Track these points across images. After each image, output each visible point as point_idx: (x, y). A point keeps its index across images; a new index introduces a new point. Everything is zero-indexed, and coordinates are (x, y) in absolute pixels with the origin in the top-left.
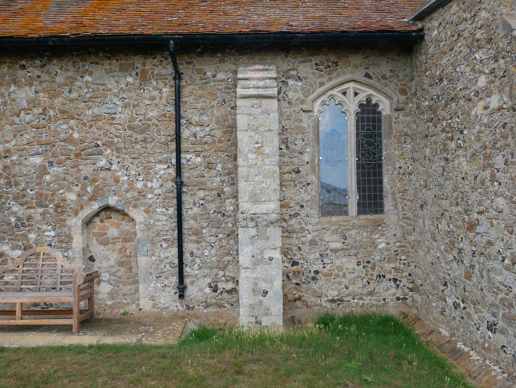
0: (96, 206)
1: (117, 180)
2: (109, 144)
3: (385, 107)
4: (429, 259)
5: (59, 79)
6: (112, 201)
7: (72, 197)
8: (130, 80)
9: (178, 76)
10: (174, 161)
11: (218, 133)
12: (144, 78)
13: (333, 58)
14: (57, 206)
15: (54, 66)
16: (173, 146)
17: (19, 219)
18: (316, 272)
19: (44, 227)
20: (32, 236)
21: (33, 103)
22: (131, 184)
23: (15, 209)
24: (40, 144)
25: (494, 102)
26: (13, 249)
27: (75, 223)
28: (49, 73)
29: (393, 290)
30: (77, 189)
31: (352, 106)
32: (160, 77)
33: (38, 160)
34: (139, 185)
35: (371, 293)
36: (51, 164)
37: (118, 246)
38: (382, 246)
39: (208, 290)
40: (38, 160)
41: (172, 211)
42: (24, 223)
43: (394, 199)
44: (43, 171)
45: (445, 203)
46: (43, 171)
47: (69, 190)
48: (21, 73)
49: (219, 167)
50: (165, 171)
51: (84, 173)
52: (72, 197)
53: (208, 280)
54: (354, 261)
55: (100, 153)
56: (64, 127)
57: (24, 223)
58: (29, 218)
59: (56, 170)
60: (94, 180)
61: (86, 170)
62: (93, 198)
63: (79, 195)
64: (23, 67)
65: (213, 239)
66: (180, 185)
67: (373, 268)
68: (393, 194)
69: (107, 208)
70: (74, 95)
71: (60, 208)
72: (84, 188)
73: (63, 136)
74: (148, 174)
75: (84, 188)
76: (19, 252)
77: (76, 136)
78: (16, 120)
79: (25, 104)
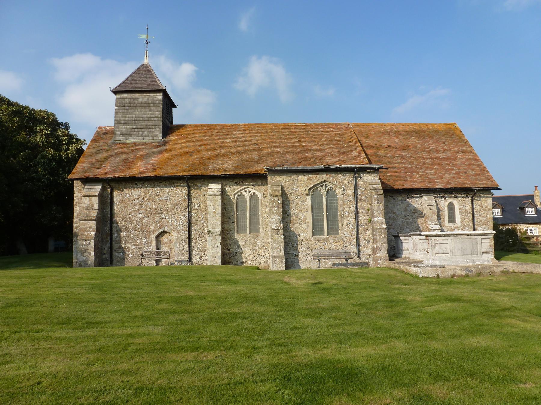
0: (160, 231)
1: (168, 222)
6: (166, 229)
7: (152, 228)
9: (189, 187)
10: (187, 215)
13: (241, 180)
14: (147, 231)
17: (134, 236)
18: (236, 253)
19: (143, 238)
20: (138, 241)
21: (140, 196)
23: (133, 232)
26: (132, 246)
29: (263, 259)
33: (141, 215)
34: (175, 224)
35: (255, 260)
36: (145, 217)
37: (168, 245)
38: (258, 244)
39: (199, 259)
40: (141, 215)
41: (187, 232)
42: (136, 237)
43: (263, 227)
44: (142, 219)
47: (151, 225)
50: (184, 219)
51: (156, 220)
52: (152, 228)
53: (198, 256)
54: (249, 249)
55: (162, 213)
56: (150, 204)
57: (136, 237)
58: (138, 235)
59: (146, 219)
60: (159, 222)
62: (160, 228)
65: (200, 242)
67: (256, 251)
68: (262, 226)
71: (148, 231)
72: (156, 225)
74: (178, 219)
75: (156, 225)
76: (134, 247)
77: (154, 207)
78: (134, 202)
79: (136, 197)
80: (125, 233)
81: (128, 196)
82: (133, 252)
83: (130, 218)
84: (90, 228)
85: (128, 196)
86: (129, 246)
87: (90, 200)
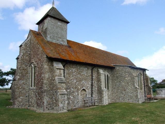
2: (84, 79)
3: (109, 75)
4: (116, 95)
5: (78, 68)
6: (84, 88)
8: (86, 69)
9: (92, 70)
10: (91, 82)
11: (96, 78)
12: (88, 69)
15: (78, 65)
16: (91, 79)
20: (74, 94)
22: (86, 85)
24: (76, 78)
25: (129, 78)
27: (80, 92)
28: (77, 66)
30: (80, 86)
31: (106, 75)
32: (90, 69)
40: (75, 81)
44: (76, 83)
45: (119, 88)
46: (76, 83)
48: (74, 66)
49: (96, 83)
50: (90, 83)
57: (73, 92)
59: (77, 83)
60: (82, 85)
61: (82, 83)
63: (80, 87)
64: (74, 65)
66: (92, 85)
69: (84, 90)
70: (80, 71)
73: (79, 77)
76: (72, 97)
79: (74, 72)
80: (69, 90)
81: (71, 71)
82: (72, 100)
83: (71, 82)
84: (63, 87)
85: (71, 71)
86: (70, 96)
87: (60, 71)
